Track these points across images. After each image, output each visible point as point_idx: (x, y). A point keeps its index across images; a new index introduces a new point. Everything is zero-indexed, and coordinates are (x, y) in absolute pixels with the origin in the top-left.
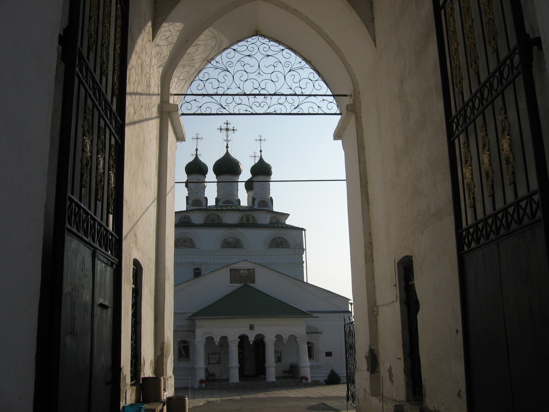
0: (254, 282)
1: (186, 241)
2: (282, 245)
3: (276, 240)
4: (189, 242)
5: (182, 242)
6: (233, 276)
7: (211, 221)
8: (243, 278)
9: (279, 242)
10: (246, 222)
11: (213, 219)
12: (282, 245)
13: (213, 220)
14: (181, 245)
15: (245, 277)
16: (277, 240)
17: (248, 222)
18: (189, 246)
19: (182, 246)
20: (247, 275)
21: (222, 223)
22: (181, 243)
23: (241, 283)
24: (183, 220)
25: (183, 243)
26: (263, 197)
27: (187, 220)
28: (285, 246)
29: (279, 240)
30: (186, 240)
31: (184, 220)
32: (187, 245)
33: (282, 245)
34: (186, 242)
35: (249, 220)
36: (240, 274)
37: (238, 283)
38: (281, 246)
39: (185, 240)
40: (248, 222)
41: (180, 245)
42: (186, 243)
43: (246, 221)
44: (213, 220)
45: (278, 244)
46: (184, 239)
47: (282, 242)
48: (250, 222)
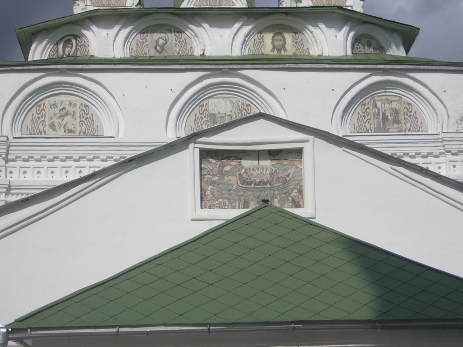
0: (297, 205)
1: (67, 114)
2: (398, 122)
3: (375, 106)
4: (77, 116)
5: (55, 115)
6: (215, 179)
7: (155, 48)
8: (253, 186)
9: (388, 113)
10: (273, 50)
11: (161, 42)
12: (398, 122)
13: (162, 47)
14: (52, 126)
15: (265, 184)
16: (379, 104)
17: (279, 51)
19: (55, 130)
20: (271, 174)
21: (192, 55)
22: (51, 118)
23: (245, 206)
24: (61, 52)
25: (56, 121)
27: (76, 49)
28: (408, 125)
29: (387, 105)
30: (68, 108)
31: (67, 50)
32: (72, 128)
33: (397, 121)
34: (68, 116)
35: (285, 43)
36: (243, 171)
37: (234, 208)
38: (396, 126)
39: (64, 108)
40: (279, 51)
41: (47, 127)
42: (68, 119)
43: (274, 47)
44: (162, 47)
45: (385, 118)
46: (60, 107)
47: (396, 112)
48: (285, 50)
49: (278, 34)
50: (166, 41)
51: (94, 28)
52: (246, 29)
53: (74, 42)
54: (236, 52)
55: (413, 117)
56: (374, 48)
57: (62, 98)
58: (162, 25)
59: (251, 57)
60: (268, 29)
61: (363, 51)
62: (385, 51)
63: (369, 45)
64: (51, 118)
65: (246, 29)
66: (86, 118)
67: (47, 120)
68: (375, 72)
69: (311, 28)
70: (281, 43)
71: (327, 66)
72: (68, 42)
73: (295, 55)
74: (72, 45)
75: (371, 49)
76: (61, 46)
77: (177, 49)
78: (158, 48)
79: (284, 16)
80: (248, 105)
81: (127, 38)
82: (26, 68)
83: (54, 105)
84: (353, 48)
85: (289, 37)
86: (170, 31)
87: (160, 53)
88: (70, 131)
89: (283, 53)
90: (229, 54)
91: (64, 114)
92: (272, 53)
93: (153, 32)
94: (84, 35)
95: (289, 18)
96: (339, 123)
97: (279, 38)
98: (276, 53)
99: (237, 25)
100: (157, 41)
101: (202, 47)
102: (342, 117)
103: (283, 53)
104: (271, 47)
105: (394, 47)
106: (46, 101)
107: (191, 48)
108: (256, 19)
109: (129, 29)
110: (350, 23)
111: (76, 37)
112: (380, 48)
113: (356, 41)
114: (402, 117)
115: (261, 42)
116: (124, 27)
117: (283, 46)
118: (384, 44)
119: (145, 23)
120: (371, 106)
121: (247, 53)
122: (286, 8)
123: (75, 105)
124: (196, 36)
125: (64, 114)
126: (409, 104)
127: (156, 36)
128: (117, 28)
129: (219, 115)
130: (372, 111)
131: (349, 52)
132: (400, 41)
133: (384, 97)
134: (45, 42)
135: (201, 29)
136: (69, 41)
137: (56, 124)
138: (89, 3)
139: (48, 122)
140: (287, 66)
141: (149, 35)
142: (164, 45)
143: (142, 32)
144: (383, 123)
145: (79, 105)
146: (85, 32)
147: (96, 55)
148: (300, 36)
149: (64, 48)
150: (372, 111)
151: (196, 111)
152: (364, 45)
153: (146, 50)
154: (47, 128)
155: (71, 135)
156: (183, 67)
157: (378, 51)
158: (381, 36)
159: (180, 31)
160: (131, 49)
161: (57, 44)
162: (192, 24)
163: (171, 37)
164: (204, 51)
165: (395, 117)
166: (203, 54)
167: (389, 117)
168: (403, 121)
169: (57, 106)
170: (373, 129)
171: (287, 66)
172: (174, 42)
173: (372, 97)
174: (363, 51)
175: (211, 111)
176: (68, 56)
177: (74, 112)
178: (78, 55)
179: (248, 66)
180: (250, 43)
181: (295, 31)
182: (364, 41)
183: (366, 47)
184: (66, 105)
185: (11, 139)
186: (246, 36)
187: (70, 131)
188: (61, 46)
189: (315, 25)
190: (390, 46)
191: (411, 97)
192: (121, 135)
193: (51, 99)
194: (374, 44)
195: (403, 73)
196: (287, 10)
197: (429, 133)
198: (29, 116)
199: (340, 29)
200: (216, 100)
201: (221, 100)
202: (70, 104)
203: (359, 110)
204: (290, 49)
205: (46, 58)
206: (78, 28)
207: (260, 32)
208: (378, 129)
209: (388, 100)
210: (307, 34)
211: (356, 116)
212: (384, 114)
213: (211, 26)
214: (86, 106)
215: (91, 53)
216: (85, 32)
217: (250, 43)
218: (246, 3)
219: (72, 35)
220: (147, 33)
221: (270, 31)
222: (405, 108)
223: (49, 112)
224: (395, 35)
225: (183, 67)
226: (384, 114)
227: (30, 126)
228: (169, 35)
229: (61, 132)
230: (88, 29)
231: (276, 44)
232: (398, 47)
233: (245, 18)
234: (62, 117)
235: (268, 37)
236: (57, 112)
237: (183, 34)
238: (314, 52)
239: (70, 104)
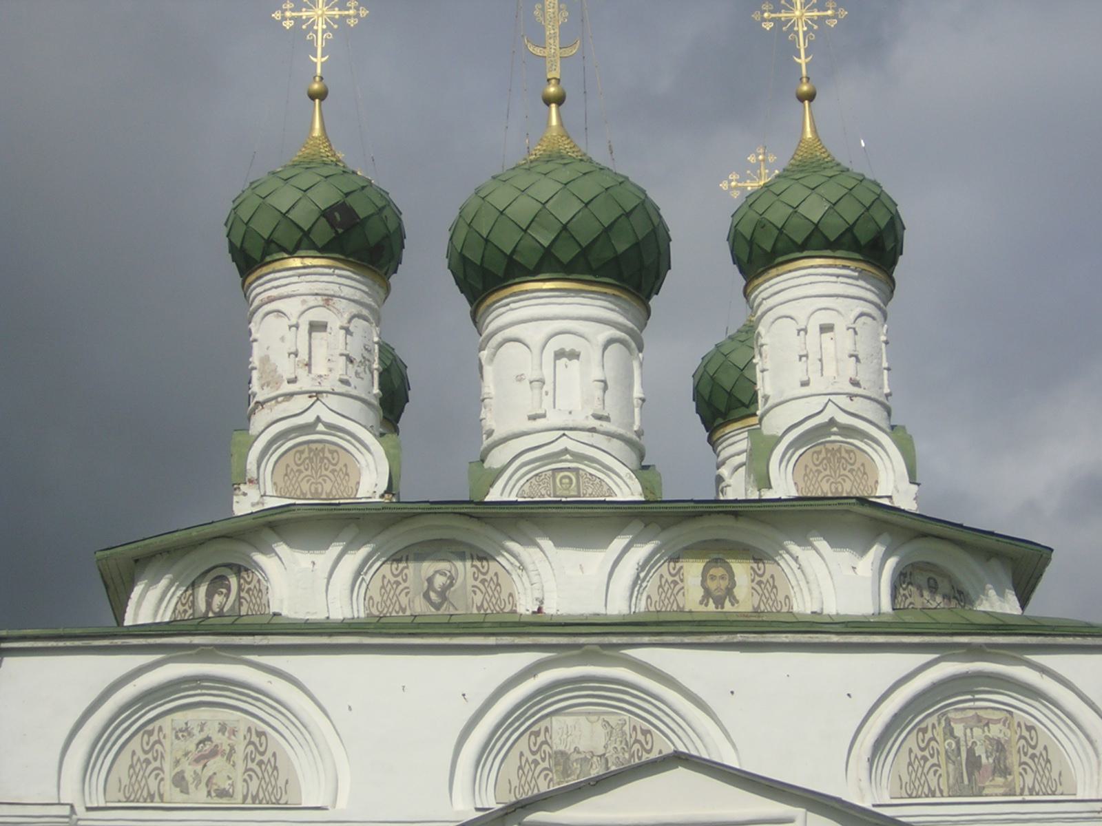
1: (214, 753)
2: (1005, 772)
3: (950, 732)
4: (239, 757)
5: (186, 754)
7: (426, 596)
9: (980, 751)
11: (439, 581)
12: (1005, 772)
13: (443, 594)
14: (179, 781)
16: (959, 730)
17: (719, 602)
18: (240, 789)
19: (185, 791)
21: (514, 612)
22: (177, 762)
24: (202, 606)
25: (189, 770)
26: (832, 422)
27: (239, 597)
29: (977, 731)
30: (218, 738)
31: (217, 600)
32: (226, 785)
34: (218, 758)
35: (734, 584)
38: (999, 780)
39: (209, 739)
40: (719, 602)
42: (216, 764)
43: (708, 593)
44: (443, 594)
45: (974, 762)
47: (999, 747)
48: (734, 601)
49: (716, 562)
50: (452, 579)
51: (282, 548)
52: (641, 552)
53: (233, 581)
54: (618, 606)
55: (1040, 758)
56: (944, 597)
57: (204, 714)
58: (442, 542)
59: (654, 618)
60: (692, 551)
61: (918, 602)
62: (972, 603)
63: (933, 589)
64: (177, 762)
65: (641, 552)
66: (260, 763)
67: (167, 766)
68: (948, 652)
69: (794, 548)
70: (724, 584)
71: (834, 639)
72: (218, 582)
73: (756, 611)
74: (229, 590)
75: (939, 599)
76: (202, 590)
77: (478, 598)
78: (433, 596)
79: (730, 521)
80: (645, 732)
81: (358, 573)
82: (119, 642)
83: (185, 732)
84: (894, 596)
85: (741, 570)
86: (462, 557)
87: (437, 607)
88: (222, 793)
89: (728, 607)
90: (603, 611)
91: (207, 752)
92: (702, 608)
93: (420, 558)
94: (258, 567)
95: (741, 524)
96: (864, 774)
97: (718, 571)
98: (711, 607)
99: (619, 543)
100: (430, 580)
101: (537, 594)
102: (871, 761)
103: (728, 607)
104: (700, 593)
105: (992, 593)
106: (166, 722)
107: (511, 595)
108: (664, 528)
109: (364, 551)
110: (886, 537)
111: (239, 570)
112: (960, 596)
113: (902, 578)
114: (1013, 759)
115: (677, 581)
116: (351, 546)
117: (729, 591)
118: (967, 584)
119: (401, 537)
120: (939, 733)
121: (642, 607)
122: (736, 501)
123: (234, 732)
124: (523, 567)
125: (207, 752)
126: (1030, 728)
127: (428, 567)
128: (335, 549)
129: (576, 756)
130: (944, 745)
131: (886, 606)
132: (1006, 579)
133: (971, 713)
134: (164, 582)
135: (533, 551)
136: (222, 578)
137: (189, 776)
138: (270, 490)
139: (169, 771)
140: (739, 638)
141: (411, 565)
142: (446, 588)
143: (396, 558)
144: (970, 775)
145: (242, 731)
146: (259, 558)
147: (284, 613)
148: (770, 568)
149: (210, 596)
150: (944, 745)
151: (523, 745)
152: (920, 588)
153: (404, 600)
154: (167, 787)
155: (224, 802)
156: (492, 641)
157: (954, 603)
158: (962, 567)
159: (484, 557)
160: (368, 599)
161: (194, 585)
162: (513, 540)
163: (464, 569)
164: (542, 602)
165: (997, 760)
166: (540, 610)
167: (984, 760)
168: (1017, 769)
169: (190, 734)
170: (944, 787)
171: (739, 638)
172: (471, 581)
173: (942, 713)
174: (918, 602)
175: (558, 745)
176: (220, 614)
177: (232, 749)
178: (244, 611)
179: (646, 639)
180: (651, 585)
181: (758, 557)
182: (921, 579)
183: (926, 594)
184: (212, 731)
185: (80, 811)
186: (642, 568)
187: (222, 793)
188: (202, 590)
189: (804, 542)
190: (983, 591)
191: (1036, 711)
192: (342, 803)
193: (179, 717)
194: (944, 586)
195: (1014, 654)
196: (737, 507)
197: (1078, 797)
198: (125, 758)
199: (863, 552)
200: (569, 720)
201: (582, 719)
202: (223, 728)
203: (912, 742)
204: (745, 598)
205: (167, 619)
206: (243, 548)
207: (675, 559)
208: (957, 790)
209: (979, 719)
210: (785, 562)
211: (904, 758)
212: (971, 752)
213: (558, 545)
214: (260, 734)
215: (274, 608)
216: (259, 558)
217: (651, 585)
218: (639, 488)
219: (229, 566)
220: (407, 560)
221: (697, 557)
222: (1022, 737)
223: (172, 747)
224: (995, 564)
225: (492, 641)
226: (971, 752)
227: (125, 781)
228: (459, 564)
229: (199, 795)
230: (268, 551)
231: (712, 585)
232: (1001, 594)
233: (638, 526)
234: (203, 759)
235: (693, 570)
236: (192, 747)
237: (493, 564)
238: (803, 605)
239: (223, 728)
